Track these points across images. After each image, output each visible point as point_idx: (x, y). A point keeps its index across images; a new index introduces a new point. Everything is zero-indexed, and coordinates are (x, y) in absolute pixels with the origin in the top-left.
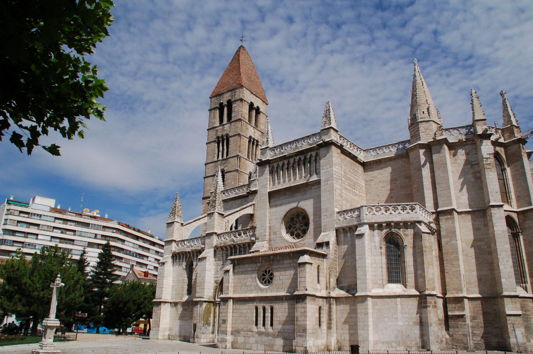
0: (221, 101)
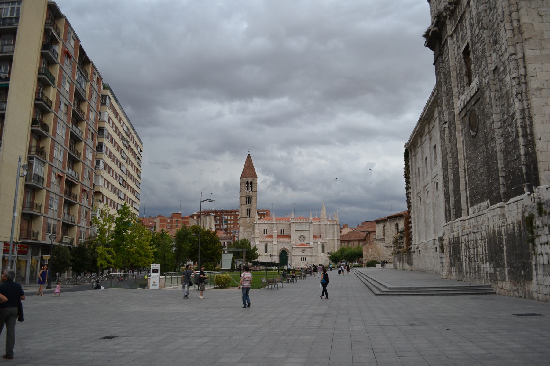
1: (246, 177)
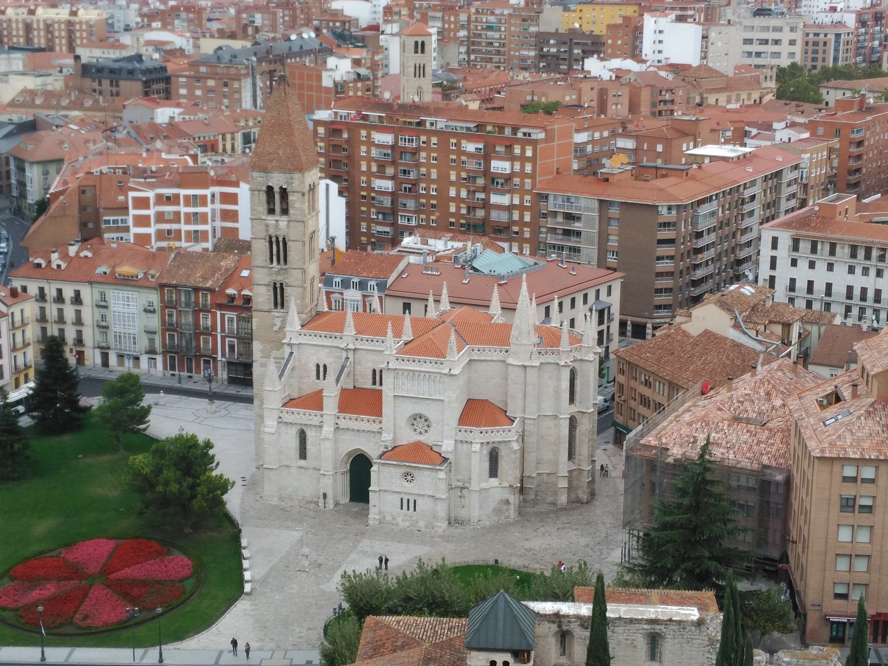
0: (270, 184)
1: (264, 170)
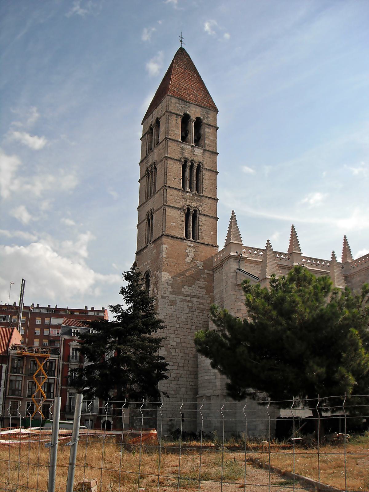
0: (188, 112)
